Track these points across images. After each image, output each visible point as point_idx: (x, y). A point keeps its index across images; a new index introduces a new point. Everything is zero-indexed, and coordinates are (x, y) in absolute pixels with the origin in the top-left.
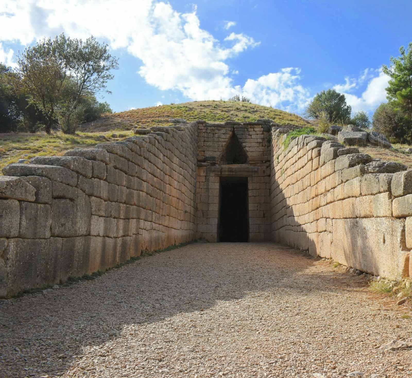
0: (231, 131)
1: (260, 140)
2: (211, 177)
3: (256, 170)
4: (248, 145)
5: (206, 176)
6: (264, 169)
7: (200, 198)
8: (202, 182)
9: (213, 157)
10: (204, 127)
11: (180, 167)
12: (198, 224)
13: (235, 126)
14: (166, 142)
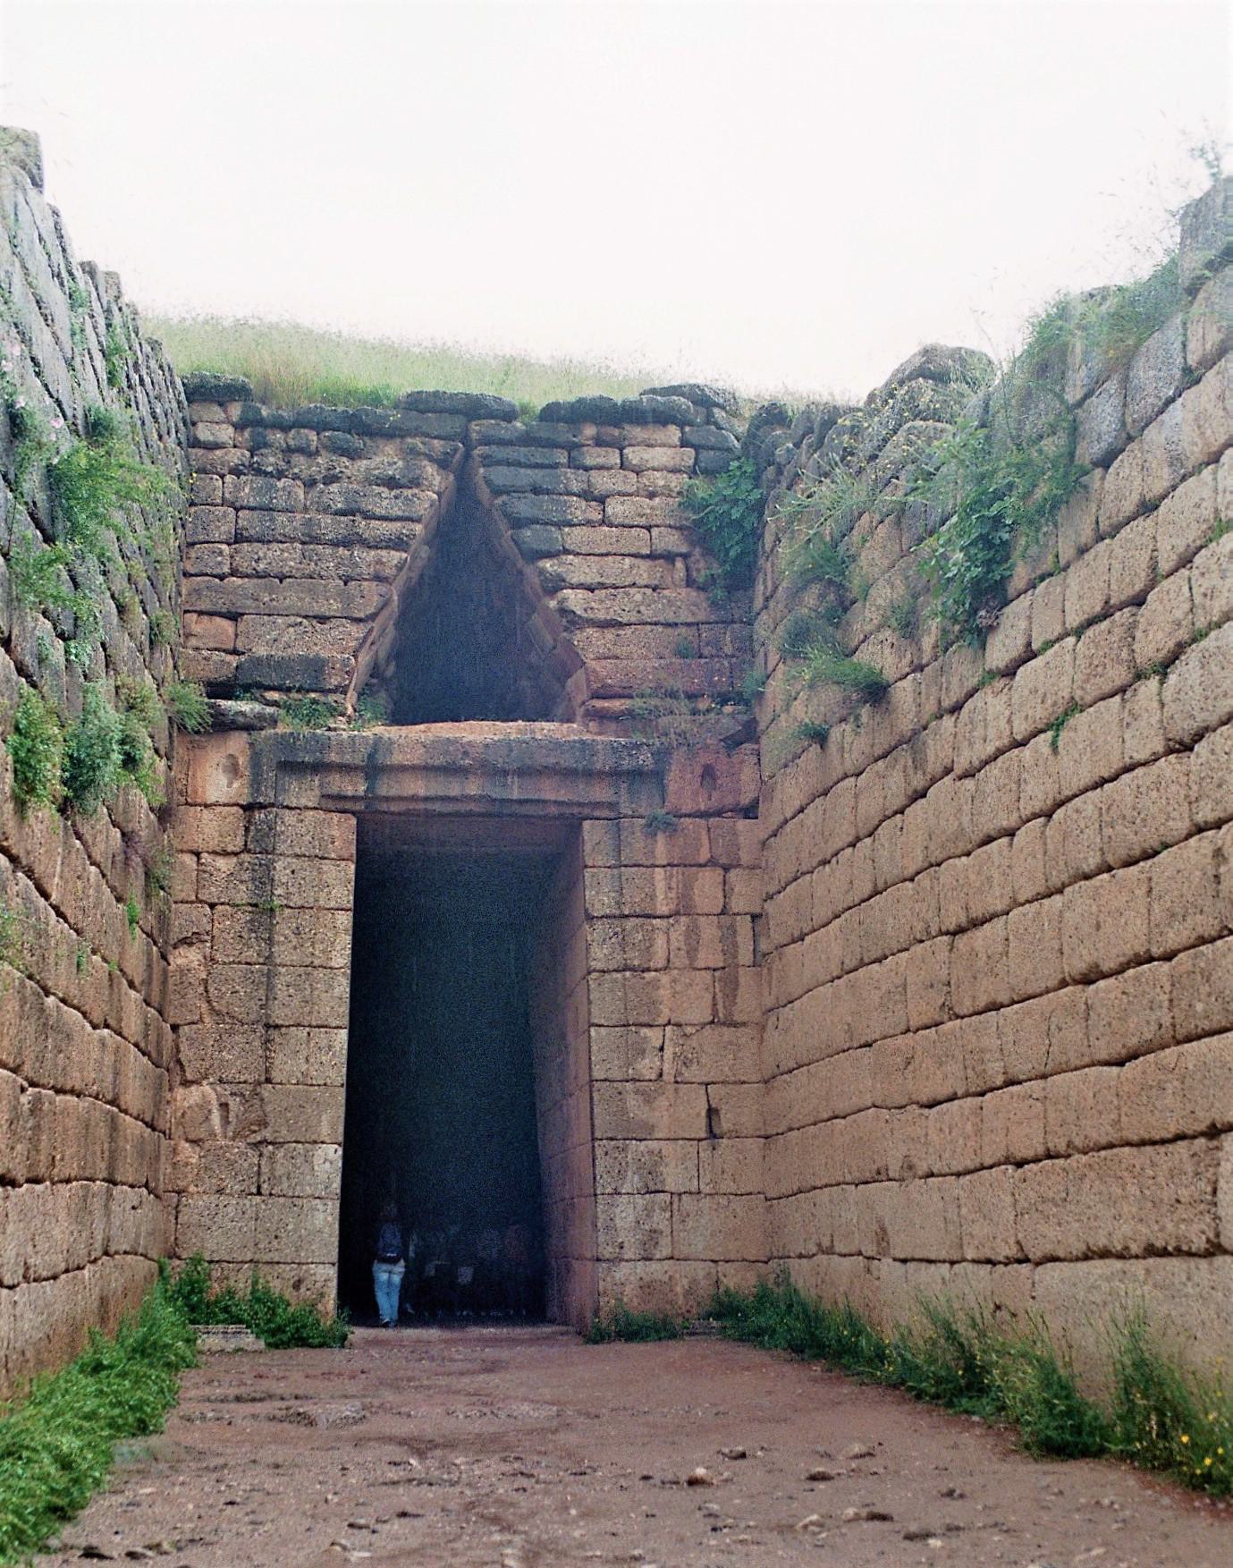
0: (443, 464)
1: (670, 541)
3: (645, 759)
4: (579, 570)
5: (248, 808)
8: (225, 854)
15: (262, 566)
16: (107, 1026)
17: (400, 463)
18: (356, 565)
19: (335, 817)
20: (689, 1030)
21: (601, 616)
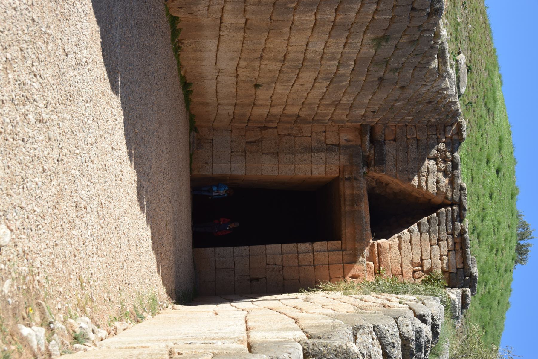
1: (427, 266)
2: (337, 157)
5: (339, 145)
6: (361, 277)
7: (289, 135)
8: (325, 139)
9: (383, 160)
10: (451, 138)
11: (355, 61)
12: (231, 131)
13: (456, 208)
14: (410, 7)
15: (410, 146)
16: (272, 101)
17: (444, 185)
18: (413, 173)
19: (338, 170)
20: (281, 272)
21: (403, 245)
